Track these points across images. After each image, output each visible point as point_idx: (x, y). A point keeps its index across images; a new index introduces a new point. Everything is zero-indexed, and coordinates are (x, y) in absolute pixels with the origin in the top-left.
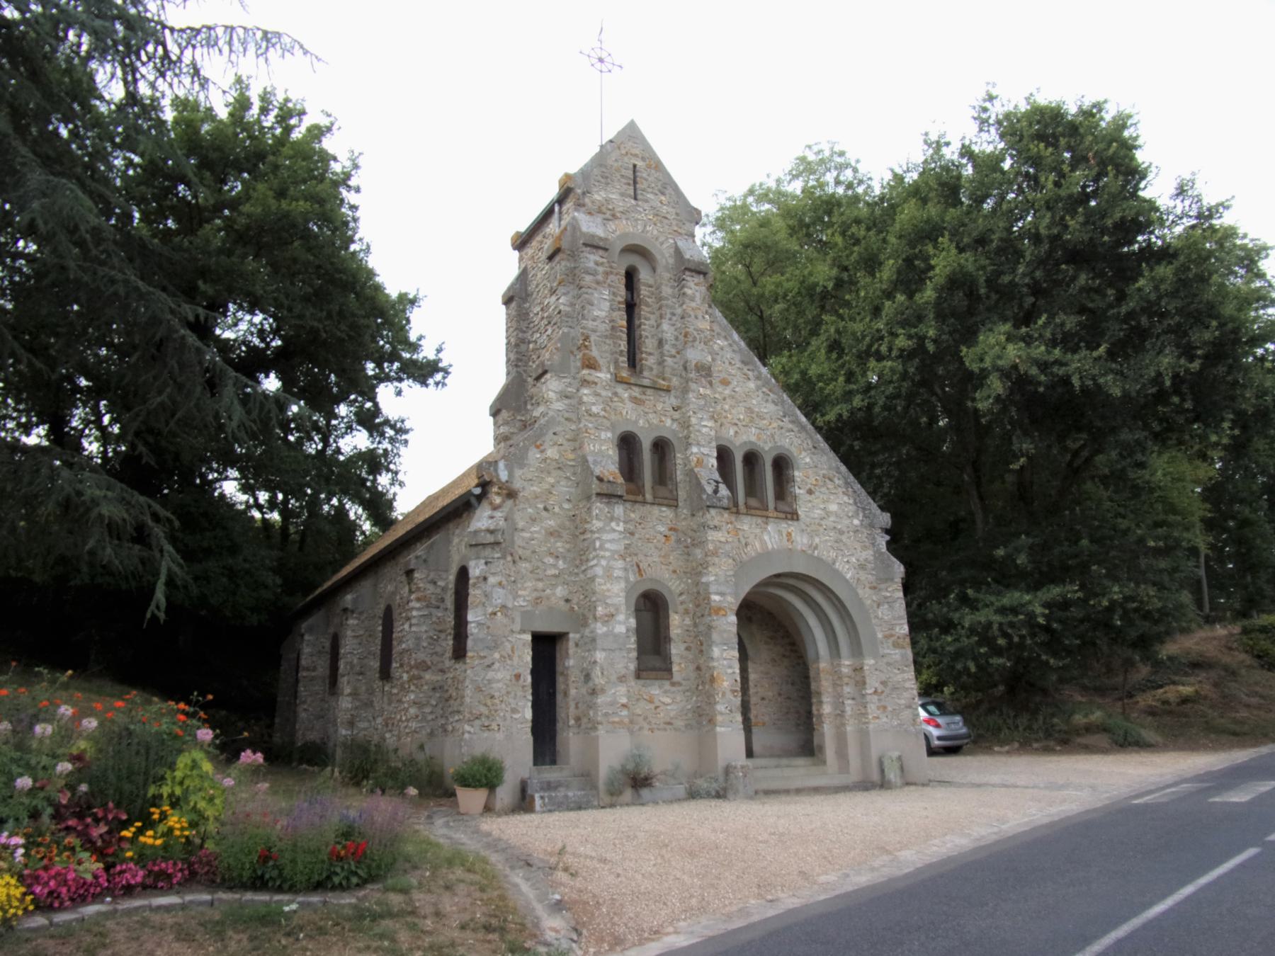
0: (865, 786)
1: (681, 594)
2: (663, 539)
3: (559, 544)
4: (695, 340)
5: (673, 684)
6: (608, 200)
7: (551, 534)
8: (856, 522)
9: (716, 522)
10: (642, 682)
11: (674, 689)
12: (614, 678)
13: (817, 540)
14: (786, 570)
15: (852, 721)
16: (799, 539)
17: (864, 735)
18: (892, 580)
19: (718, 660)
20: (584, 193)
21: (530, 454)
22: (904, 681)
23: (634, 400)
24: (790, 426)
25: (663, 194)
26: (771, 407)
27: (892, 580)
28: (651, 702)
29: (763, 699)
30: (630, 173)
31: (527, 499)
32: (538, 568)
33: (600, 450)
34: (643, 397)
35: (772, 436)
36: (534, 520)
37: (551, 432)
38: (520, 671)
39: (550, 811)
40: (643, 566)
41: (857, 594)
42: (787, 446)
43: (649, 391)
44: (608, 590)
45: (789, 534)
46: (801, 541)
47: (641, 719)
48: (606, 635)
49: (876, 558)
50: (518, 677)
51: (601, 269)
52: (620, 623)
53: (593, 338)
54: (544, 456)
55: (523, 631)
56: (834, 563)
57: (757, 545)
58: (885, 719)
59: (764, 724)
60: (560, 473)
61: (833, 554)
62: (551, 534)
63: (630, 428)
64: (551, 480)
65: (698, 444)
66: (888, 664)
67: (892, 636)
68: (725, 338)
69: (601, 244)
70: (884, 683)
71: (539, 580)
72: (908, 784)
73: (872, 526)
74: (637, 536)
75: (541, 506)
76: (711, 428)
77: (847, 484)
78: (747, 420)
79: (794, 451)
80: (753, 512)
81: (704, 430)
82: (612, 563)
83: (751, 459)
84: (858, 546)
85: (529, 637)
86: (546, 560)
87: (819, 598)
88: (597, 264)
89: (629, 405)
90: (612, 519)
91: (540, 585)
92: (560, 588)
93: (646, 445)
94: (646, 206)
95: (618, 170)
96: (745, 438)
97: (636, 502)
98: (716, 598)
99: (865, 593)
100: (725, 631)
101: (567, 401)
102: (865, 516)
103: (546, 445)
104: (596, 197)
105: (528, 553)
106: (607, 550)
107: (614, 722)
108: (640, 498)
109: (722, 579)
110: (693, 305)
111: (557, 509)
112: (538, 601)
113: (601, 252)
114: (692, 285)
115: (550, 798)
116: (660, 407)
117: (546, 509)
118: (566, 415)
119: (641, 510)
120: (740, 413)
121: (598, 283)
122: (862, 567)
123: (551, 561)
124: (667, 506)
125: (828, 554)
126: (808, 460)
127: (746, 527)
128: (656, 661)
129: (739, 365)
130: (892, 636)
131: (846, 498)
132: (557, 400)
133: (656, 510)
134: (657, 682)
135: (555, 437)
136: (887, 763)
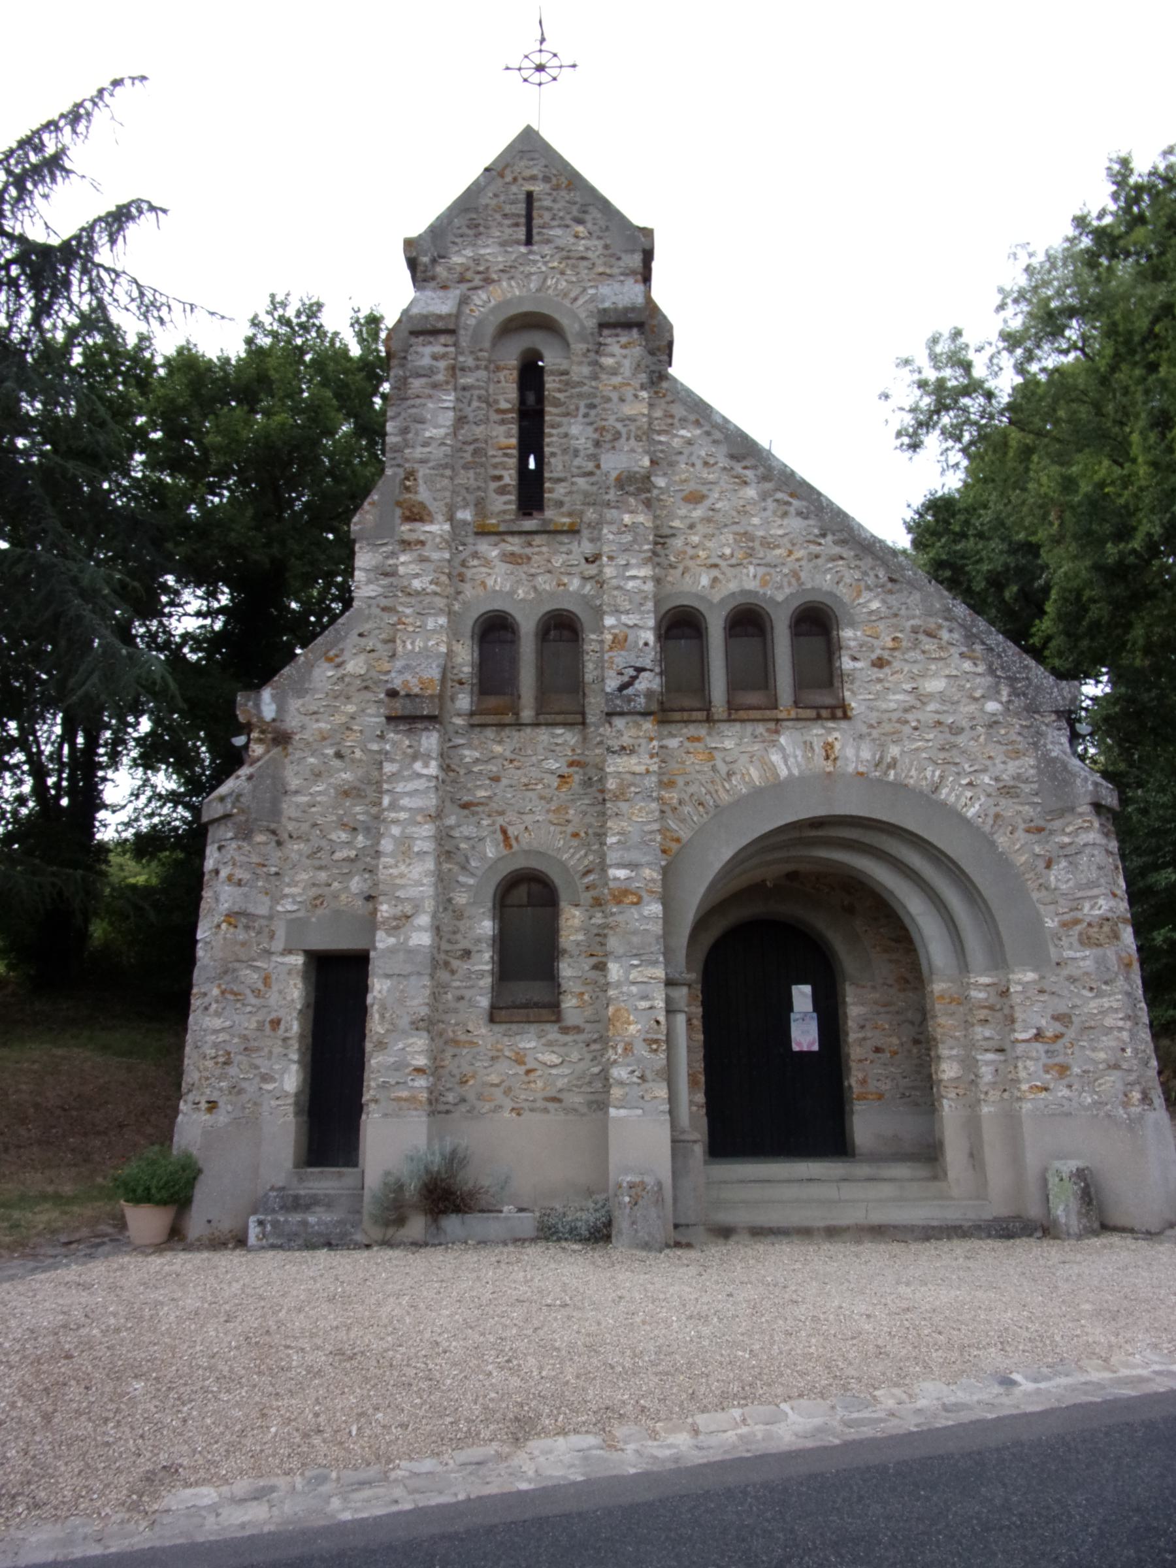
0: (1011, 1228)
1: (588, 872)
2: (555, 782)
3: (358, 809)
4: (617, 436)
5: (565, 1030)
6: (477, 260)
7: (346, 794)
8: (992, 706)
9: (626, 740)
10: (499, 1028)
11: (568, 1038)
12: (404, 1023)
13: (894, 751)
14: (821, 811)
15: (994, 1095)
16: (850, 752)
17: (1011, 1120)
18: (1072, 810)
19: (618, 984)
20: (434, 261)
21: (317, 672)
22: (1104, 1012)
23: (512, 559)
24: (837, 550)
25: (580, 222)
26: (795, 524)
27: (1072, 810)
28: (520, 1061)
29: (877, 1050)
30: (521, 208)
31: (308, 744)
32: (320, 849)
33: (426, 648)
34: (528, 551)
35: (795, 574)
36: (318, 775)
37: (356, 632)
38: (281, 1013)
39: (273, 1247)
40: (512, 831)
41: (993, 844)
42: (826, 587)
43: (538, 540)
44: (402, 876)
45: (828, 747)
46: (854, 753)
47: (498, 1092)
48: (392, 951)
49: (1040, 772)
50: (275, 1023)
51: (442, 364)
52: (420, 928)
53: (422, 471)
54: (341, 672)
55: (288, 951)
56: (936, 789)
57: (754, 773)
58: (1065, 1092)
59: (880, 1097)
60: (369, 695)
61: (932, 773)
62: (346, 794)
63: (497, 605)
64: (351, 708)
65: (617, 611)
66: (1072, 980)
67: (1076, 922)
68: (697, 423)
69: (440, 325)
70: (1062, 1018)
71: (320, 868)
72: (1106, 1228)
73: (1032, 710)
74: (504, 782)
75: (330, 751)
76: (644, 580)
77: (970, 638)
78: (739, 554)
79: (842, 591)
80: (742, 714)
81: (631, 585)
82: (410, 830)
83: (748, 621)
84: (997, 752)
85: (298, 960)
86: (333, 836)
87: (915, 860)
88: (435, 357)
89: (502, 568)
90: (415, 757)
91: (323, 876)
92: (356, 878)
93: (527, 626)
94: (547, 249)
95: (498, 209)
96: (733, 586)
97: (502, 726)
98: (622, 873)
99: (1017, 846)
100: (635, 932)
101: (385, 581)
102: (1015, 693)
103: (346, 655)
104: (456, 259)
105: (305, 827)
106: (403, 809)
107: (399, 1099)
108: (509, 718)
109: (636, 838)
110: (616, 380)
111: (358, 754)
112: (317, 902)
113: (443, 339)
114: (616, 349)
115: (275, 1224)
116: (558, 561)
117: (339, 755)
118: (384, 602)
119: (516, 738)
120: (725, 544)
121: (435, 386)
122: (1007, 791)
123: (344, 836)
124: (564, 724)
125: (919, 773)
126: (875, 605)
127: (729, 744)
128: (534, 991)
129: (723, 462)
130: (1076, 922)
131: (967, 665)
132: (369, 582)
133: (543, 735)
134: (533, 1028)
135: (363, 641)
136: (1053, 1181)
